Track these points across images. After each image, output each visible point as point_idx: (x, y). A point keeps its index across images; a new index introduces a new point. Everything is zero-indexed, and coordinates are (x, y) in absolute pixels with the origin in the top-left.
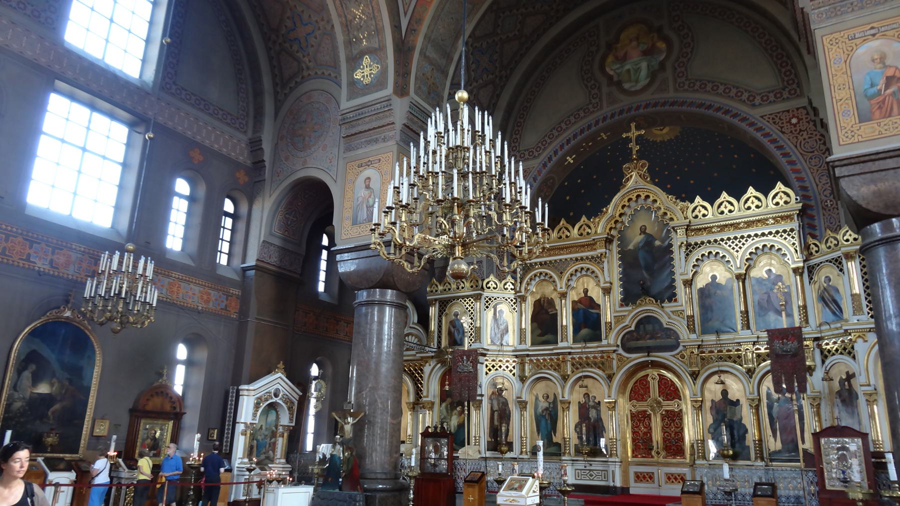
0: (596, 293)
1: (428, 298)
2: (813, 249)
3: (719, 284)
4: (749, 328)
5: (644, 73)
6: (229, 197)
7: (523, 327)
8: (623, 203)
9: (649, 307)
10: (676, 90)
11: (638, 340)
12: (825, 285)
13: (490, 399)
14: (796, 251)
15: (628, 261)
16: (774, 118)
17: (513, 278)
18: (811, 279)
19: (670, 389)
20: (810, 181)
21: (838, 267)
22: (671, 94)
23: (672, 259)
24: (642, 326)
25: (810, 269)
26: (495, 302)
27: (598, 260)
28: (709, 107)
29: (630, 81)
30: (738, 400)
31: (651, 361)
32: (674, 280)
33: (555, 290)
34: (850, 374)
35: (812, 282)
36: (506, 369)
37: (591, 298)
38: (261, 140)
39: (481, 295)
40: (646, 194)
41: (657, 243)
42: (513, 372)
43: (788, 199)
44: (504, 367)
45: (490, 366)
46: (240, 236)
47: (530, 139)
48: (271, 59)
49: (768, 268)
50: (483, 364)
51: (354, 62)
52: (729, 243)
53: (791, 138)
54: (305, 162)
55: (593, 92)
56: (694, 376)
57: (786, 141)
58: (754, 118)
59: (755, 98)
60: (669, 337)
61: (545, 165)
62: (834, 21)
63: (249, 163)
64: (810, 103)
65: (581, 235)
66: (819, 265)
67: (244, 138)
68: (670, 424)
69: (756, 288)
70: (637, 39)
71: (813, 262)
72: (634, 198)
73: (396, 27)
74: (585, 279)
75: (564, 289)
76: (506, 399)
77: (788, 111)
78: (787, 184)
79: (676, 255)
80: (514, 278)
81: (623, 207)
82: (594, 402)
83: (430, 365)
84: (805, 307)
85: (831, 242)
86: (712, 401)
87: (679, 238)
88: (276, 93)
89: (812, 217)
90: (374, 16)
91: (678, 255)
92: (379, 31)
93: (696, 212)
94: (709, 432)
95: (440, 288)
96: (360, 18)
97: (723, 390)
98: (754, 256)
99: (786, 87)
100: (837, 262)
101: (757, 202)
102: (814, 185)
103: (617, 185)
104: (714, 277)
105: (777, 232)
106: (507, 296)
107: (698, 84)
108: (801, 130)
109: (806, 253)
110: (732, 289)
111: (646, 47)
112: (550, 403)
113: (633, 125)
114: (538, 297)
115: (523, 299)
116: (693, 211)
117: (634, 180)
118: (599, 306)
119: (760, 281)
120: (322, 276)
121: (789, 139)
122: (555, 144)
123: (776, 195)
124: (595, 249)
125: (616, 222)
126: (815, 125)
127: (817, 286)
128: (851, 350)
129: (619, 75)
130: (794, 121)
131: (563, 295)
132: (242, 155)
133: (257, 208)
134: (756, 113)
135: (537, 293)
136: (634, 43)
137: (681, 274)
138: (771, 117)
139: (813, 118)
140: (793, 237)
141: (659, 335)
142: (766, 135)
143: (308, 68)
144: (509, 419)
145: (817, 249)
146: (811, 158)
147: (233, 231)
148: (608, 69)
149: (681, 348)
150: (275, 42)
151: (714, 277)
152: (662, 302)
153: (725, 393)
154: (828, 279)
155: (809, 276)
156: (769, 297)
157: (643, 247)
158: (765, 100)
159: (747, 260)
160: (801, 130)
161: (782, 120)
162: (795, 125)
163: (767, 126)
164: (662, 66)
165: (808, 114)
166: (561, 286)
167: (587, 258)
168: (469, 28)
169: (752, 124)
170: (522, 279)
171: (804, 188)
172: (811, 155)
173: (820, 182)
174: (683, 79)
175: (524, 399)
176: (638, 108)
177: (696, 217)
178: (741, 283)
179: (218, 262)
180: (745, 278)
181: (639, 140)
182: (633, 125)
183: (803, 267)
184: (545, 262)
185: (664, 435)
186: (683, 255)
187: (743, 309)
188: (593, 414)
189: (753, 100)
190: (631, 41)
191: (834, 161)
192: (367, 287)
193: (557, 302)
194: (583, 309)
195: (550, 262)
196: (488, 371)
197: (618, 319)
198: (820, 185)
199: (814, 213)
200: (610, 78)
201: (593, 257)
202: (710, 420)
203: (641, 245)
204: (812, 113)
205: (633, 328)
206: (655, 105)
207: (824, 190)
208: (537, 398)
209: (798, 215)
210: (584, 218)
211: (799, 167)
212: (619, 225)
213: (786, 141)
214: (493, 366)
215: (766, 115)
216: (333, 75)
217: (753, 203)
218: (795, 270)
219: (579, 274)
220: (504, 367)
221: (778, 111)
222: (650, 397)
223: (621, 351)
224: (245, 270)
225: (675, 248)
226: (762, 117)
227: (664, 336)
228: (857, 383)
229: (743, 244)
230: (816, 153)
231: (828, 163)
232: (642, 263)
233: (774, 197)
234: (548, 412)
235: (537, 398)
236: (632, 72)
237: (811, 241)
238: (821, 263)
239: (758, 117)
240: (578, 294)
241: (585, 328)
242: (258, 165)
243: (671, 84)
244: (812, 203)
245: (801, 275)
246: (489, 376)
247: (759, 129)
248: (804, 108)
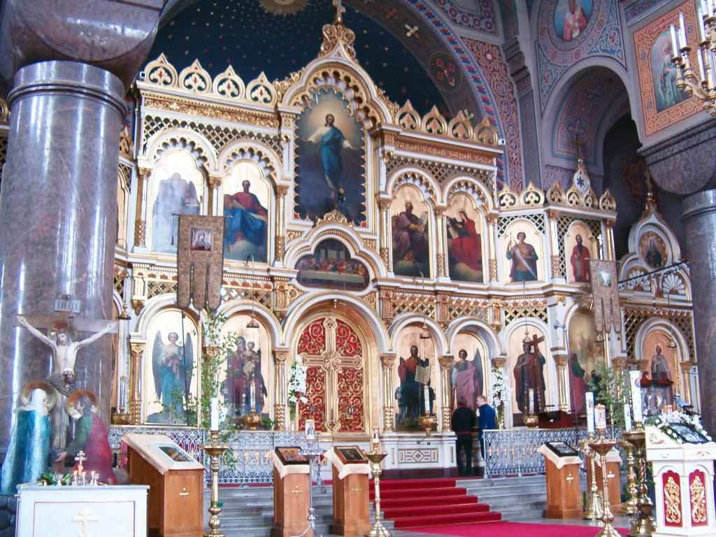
2: (507, 200)
3: (416, 217)
4: (446, 277)
7: (143, 218)
9: (335, 225)
11: (317, 269)
12: (518, 242)
14: (493, 197)
15: (307, 159)
16: (472, 44)
18: (502, 232)
19: (349, 342)
21: (537, 225)
24: (323, 251)
25: (502, 221)
30: (427, 360)
31: (339, 300)
34: (538, 337)
35: (502, 235)
37: (254, 197)
41: (346, 144)
53: (486, 74)
56: (388, 323)
57: (480, 72)
58: (456, 36)
59: (456, 14)
60: (356, 271)
66: (512, 219)
68: (348, 388)
71: (504, 215)
77: (485, 44)
82: (251, 350)
84: (496, 260)
85: (532, 197)
86: (401, 359)
94: (396, 398)
97: (413, 346)
99: (483, 18)
100: (537, 220)
102: (503, 133)
110: (426, 227)
112: (180, 348)
116: (401, 117)
118: (265, 212)
119: (453, 222)
121: (484, 74)
127: (508, 240)
128: (543, 313)
130: (489, 57)
134: (459, 31)
138: (471, 42)
139: (505, 62)
141: (345, 267)
145: (512, 201)
146: (501, 102)
149: (371, 288)
153: (414, 351)
154: (522, 236)
155: (499, 228)
157: (328, 144)
161: (479, 50)
163: (466, 51)
172: (502, 99)
173: (508, 131)
185: (340, 401)
187: (441, 252)
188: (249, 367)
189: (455, 16)
192: (87, 57)
194: (242, 211)
197: (293, 234)
198: (508, 134)
202: (397, 383)
203: (326, 140)
205: (312, 252)
207: (511, 142)
208: (158, 339)
210: (263, 76)
211: (491, 107)
213: (480, 72)
215: (465, 38)
221: (476, 39)
222: (324, 349)
223: (294, 282)
226: (462, 38)
227: (350, 269)
228: (544, 349)
230: (505, 99)
234: (176, 361)
235: (158, 339)
238: (516, 217)
239: (459, 37)
241: (243, 239)
245: (494, 226)
248: (498, 47)
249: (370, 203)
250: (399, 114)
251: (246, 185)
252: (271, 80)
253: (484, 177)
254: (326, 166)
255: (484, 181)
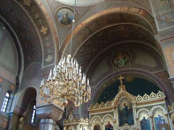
0: (112, 123)
1: (63, 125)
5: (123, 63)
6: (8, 92)
8: (119, 97)
10: (132, 67)
15: (121, 114)
16: (157, 74)
17: (88, 119)
20: (167, 91)
22: (130, 69)
23: (133, 113)
26: (83, 126)
27: (112, 113)
28: (140, 72)
29: (120, 65)
32: (133, 119)
33: (100, 122)
37: (110, 124)
38: (19, 77)
39: (79, 124)
40: (125, 94)
41: (129, 108)
43: (162, 95)
46: (10, 104)
47: (94, 80)
48: (24, 56)
49: (158, 114)
51: (46, 56)
52: (148, 107)
54: (30, 83)
55: (110, 68)
61: (98, 87)
62: (166, 46)
63: (15, 83)
64: (165, 70)
65: (107, 106)
67: (15, 77)
69: (156, 120)
70: (121, 55)
71: (170, 112)
72: (122, 95)
73: (58, 48)
74: (109, 119)
75: (103, 122)
77: (160, 73)
78: (161, 91)
79: (134, 111)
80: (89, 119)
81: (119, 98)
87: (134, 107)
88: (25, 65)
89: (169, 100)
90: (52, 45)
91: (134, 111)
92: (53, 49)
93: (138, 99)
95: (67, 122)
96: (49, 46)
98: (155, 111)
101: (154, 96)
103: (117, 92)
104: (144, 118)
105: (160, 104)
106: (86, 124)
107: (137, 66)
108: (164, 77)
109: (168, 110)
110: (149, 122)
111: (123, 57)
113: (121, 76)
114: (95, 125)
115: (91, 125)
116: (138, 99)
117: (122, 90)
118: (113, 127)
119: (156, 118)
120: (33, 118)
122: (101, 81)
123: (159, 94)
124: (111, 110)
125: (117, 102)
126: (167, 76)
129: (117, 63)
131: (102, 124)
132: (14, 82)
133: (16, 96)
134: (152, 73)
135: (95, 123)
136: (121, 56)
137: (135, 117)
140: (164, 106)
142: (155, 79)
143: (34, 59)
147: (8, 102)
148: (114, 62)
150: (26, 52)
151: (144, 118)
152: (130, 125)
156: (159, 123)
158: (154, 70)
159: (153, 112)
160: (164, 77)
162: (162, 76)
164: (128, 61)
165: (165, 73)
166: (102, 121)
167: (109, 113)
168: (77, 50)
169: (151, 76)
170: (91, 119)
171: (166, 92)
172: (167, 84)
174: (133, 65)
176: (122, 72)
177: (139, 100)
178: (151, 119)
179: (2, 111)
180: (152, 118)
181: (123, 80)
182: (121, 76)
183: (168, 114)
184: (98, 114)
186: (135, 111)
187: (153, 126)
190: (120, 55)
191: (170, 79)
193: (101, 126)
195: (99, 114)
199: (169, 99)
200: (115, 64)
201: (111, 112)
204: (166, 72)
206: (127, 71)
209: (165, 99)
210: (108, 101)
212: (118, 103)
213: (160, 80)
216: (40, 60)
217: (153, 96)
218: (166, 115)
219: (107, 117)
224: (10, 113)
225: (133, 109)
229: (151, 108)
231: (169, 80)
232: (125, 114)
233: (158, 95)
236: (120, 63)
237: (169, 106)
240: (107, 124)
242: (17, 84)
243: (130, 65)
244: (168, 96)
245: (167, 116)
247: (153, 77)
248: (164, 72)
249: (135, 120)
250: (137, 99)
251: (109, 123)
252: (110, 102)
253: (162, 105)
254: (125, 114)
255: (162, 106)
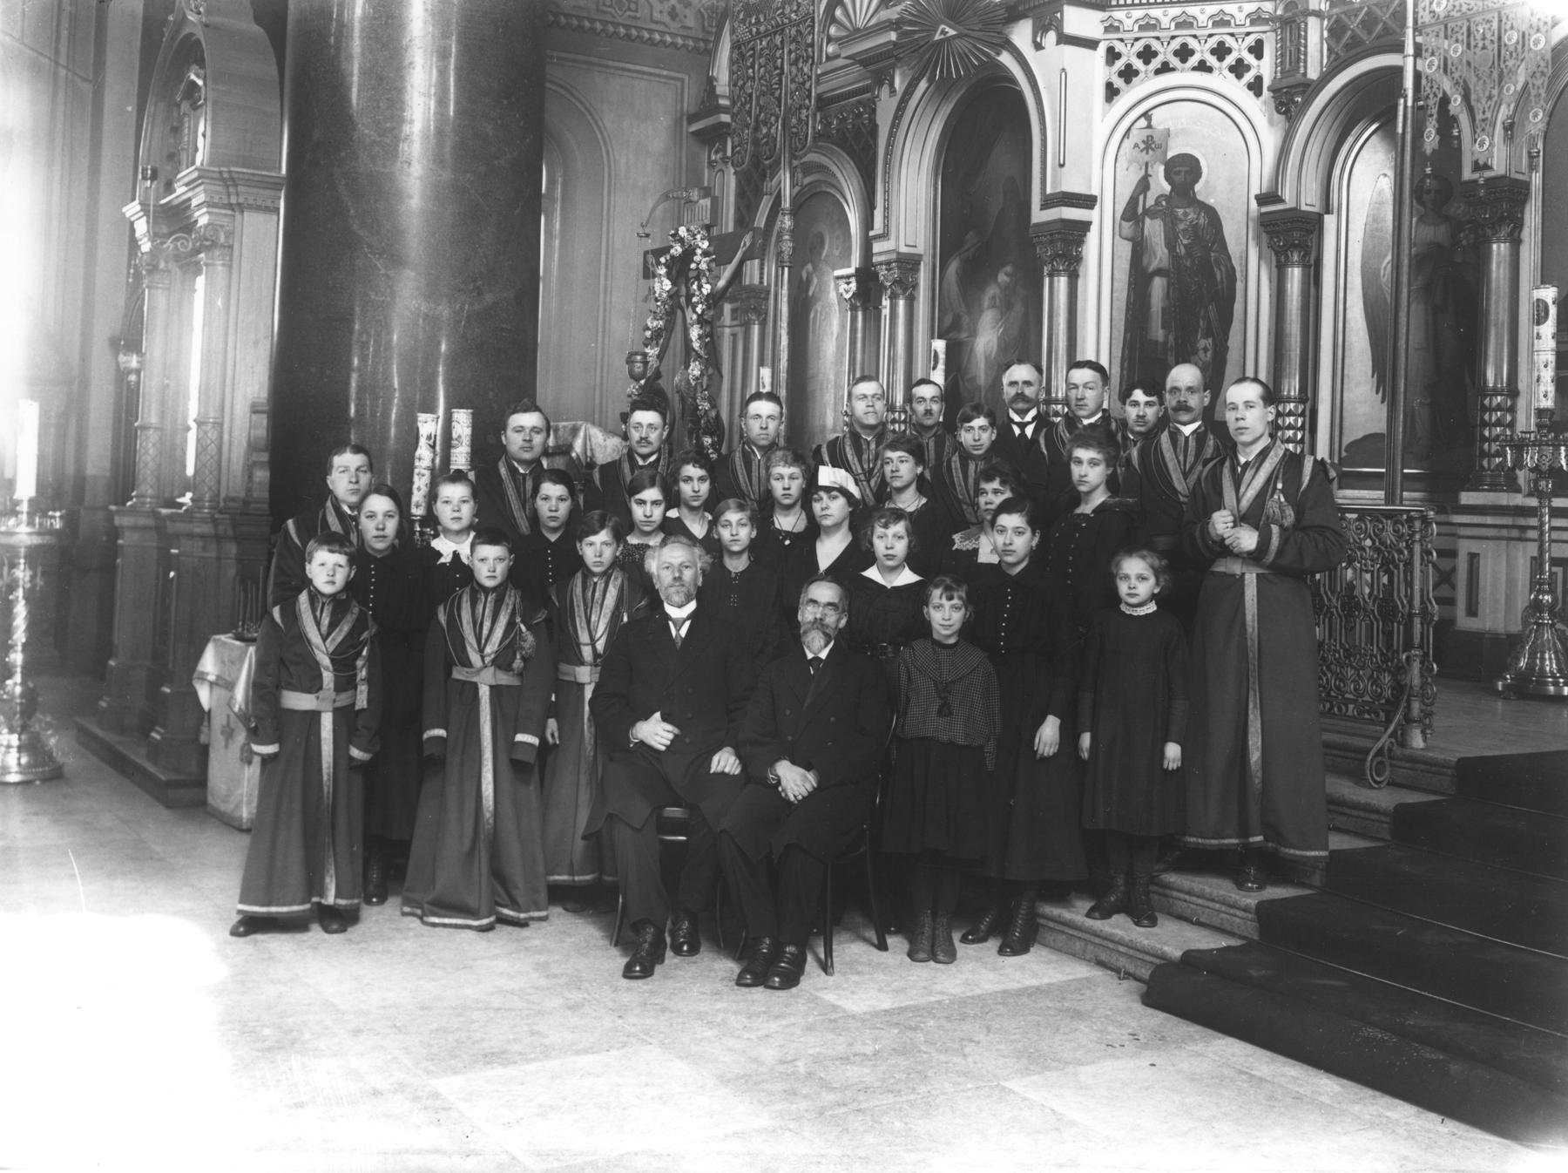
13: (1132, 213)
36: (1212, 61)
42: (1249, 77)
44: (1202, 52)
45: (1129, 55)
50: (1091, 44)
76: (1211, 213)
83: (893, 91)
144: (1226, 318)
175: (1289, 202)
196: (1118, 82)
214: (1147, 55)
220: (1202, 52)
246: (1123, 102)
